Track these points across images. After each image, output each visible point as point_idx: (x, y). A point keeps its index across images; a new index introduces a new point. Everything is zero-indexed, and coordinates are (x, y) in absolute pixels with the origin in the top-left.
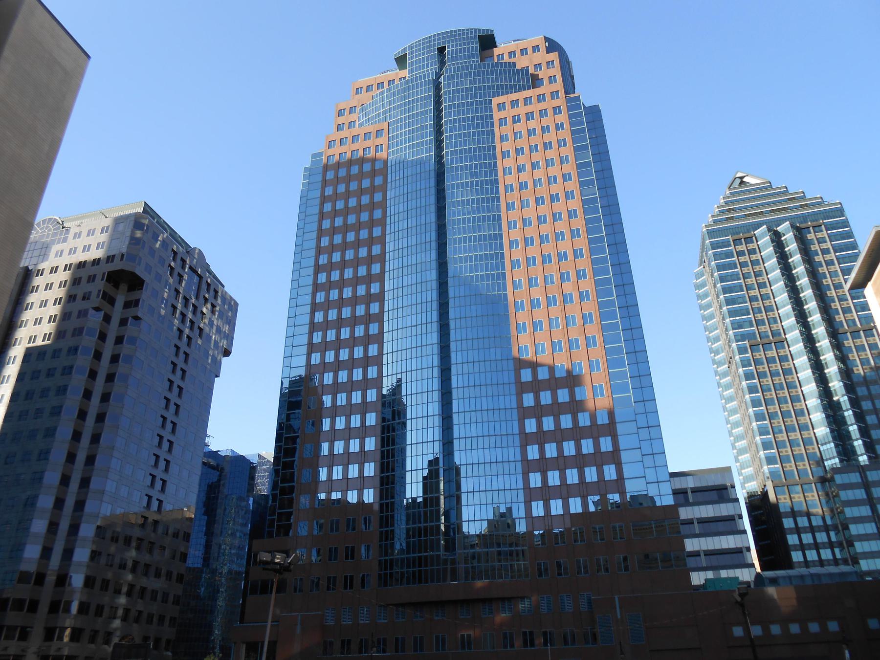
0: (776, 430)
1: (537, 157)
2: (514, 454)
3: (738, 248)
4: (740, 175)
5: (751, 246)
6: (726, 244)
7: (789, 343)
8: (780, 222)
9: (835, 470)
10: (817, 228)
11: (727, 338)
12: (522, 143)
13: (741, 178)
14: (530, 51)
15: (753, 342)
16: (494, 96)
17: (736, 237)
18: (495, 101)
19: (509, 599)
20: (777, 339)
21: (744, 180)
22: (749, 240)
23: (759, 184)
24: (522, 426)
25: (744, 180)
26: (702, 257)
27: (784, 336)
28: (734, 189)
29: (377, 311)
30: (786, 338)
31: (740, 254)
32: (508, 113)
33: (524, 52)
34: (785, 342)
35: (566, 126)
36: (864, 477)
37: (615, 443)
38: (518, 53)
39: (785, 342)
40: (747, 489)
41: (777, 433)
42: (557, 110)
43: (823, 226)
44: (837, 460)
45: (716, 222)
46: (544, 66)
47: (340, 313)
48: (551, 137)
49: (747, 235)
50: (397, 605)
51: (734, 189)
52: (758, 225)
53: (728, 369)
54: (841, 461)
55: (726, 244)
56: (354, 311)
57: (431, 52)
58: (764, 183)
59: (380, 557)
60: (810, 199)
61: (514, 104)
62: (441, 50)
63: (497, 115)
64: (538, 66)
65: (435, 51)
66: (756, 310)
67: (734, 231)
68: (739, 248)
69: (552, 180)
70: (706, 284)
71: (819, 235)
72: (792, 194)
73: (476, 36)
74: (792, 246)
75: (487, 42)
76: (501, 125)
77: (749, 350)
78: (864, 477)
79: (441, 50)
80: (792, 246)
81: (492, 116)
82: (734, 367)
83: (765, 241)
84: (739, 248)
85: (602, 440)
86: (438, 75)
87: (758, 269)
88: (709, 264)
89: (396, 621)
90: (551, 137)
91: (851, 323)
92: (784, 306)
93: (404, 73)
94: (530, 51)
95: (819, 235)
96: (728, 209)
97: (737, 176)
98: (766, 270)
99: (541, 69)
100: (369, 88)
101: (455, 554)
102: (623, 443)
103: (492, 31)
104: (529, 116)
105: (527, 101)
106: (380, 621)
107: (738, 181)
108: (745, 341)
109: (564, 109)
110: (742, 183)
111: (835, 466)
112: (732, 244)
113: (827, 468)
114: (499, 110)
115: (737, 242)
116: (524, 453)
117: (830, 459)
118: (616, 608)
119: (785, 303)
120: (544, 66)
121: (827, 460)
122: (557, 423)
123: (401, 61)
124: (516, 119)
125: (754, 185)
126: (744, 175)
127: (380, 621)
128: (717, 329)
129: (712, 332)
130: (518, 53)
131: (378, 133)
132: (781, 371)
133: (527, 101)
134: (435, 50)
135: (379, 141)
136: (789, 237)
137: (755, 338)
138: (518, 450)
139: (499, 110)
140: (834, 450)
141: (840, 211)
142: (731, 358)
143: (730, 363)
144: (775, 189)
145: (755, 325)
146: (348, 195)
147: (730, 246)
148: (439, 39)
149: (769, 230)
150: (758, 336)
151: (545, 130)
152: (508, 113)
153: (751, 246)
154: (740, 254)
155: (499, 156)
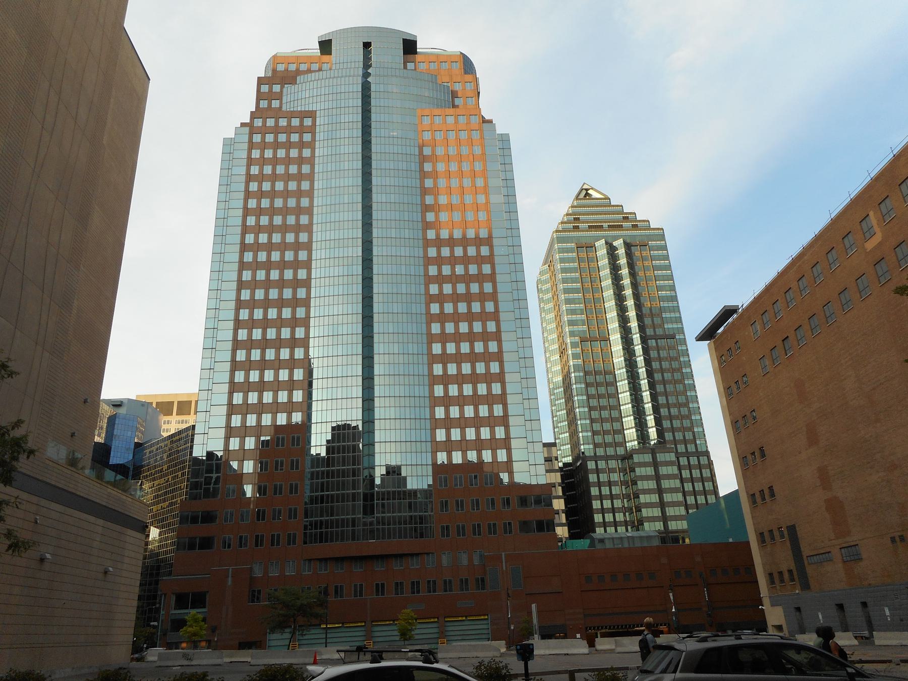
2: (425, 435)
7: (611, 342)
9: (634, 451)
13: (587, 190)
19: (417, 555)
23: (601, 199)
24: (433, 413)
25: (588, 192)
27: (608, 337)
28: (581, 199)
29: (304, 296)
30: (609, 338)
36: (654, 458)
37: (507, 432)
44: (636, 443)
47: (267, 294)
50: (320, 560)
54: (639, 443)
56: (281, 293)
62: (367, 45)
72: (626, 213)
74: (623, 261)
75: (410, 46)
78: (654, 458)
79: (367, 45)
80: (623, 261)
83: (602, 252)
85: (497, 429)
86: (366, 75)
89: (319, 572)
96: (574, 221)
97: (584, 187)
102: (513, 432)
106: (304, 573)
107: (584, 192)
111: (634, 448)
113: (628, 449)
116: (433, 435)
117: (631, 441)
118: (502, 562)
121: (628, 442)
122: (462, 412)
123: (325, 46)
126: (588, 187)
127: (304, 573)
136: (621, 252)
138: (429, 432)
140: (635, 434)
141: (662, 237)
142: (564, 349)
143: (562, 353)
144: (614, 206)
146: (274, 178)
149: (607, 243)
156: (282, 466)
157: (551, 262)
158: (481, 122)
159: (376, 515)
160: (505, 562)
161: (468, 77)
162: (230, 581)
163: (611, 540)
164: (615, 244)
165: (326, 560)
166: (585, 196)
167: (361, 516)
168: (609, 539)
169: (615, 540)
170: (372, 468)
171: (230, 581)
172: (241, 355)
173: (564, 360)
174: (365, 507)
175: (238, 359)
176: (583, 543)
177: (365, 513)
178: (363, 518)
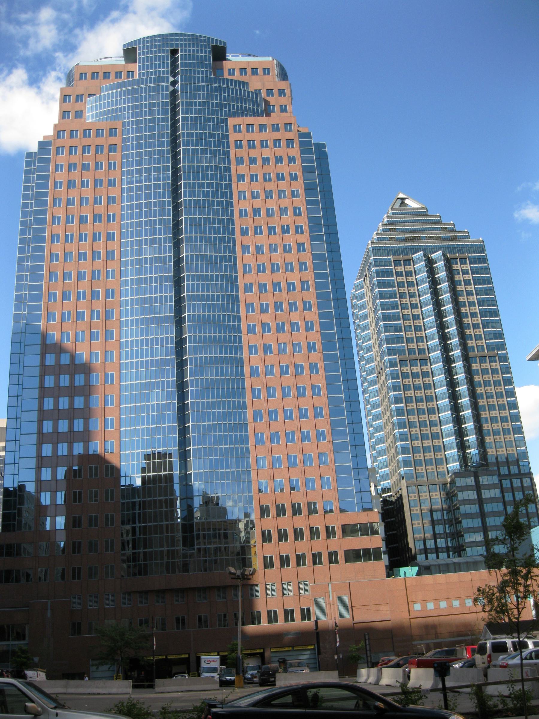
0: (413, 438)
1: (271, 186)
3: (397, 269)
4: (401, 196)
5: (408, 268)
6: (387, 263)
7: (432, 361)
8: (435, 249)
10: (463, 260)
11: (380, 351)
12: (257, 169)
13: (403, 199)
14: (260, 72)
15: (402, 357)
16: (230, 116)
17: (397, 258)
18: (232, 121)
20: (422, 356)
21: (407, 201)
22: (407, 262)
26: (363, 270)
28: (396, 209)
30: (429, 357)
31: (399, 274)
32: (244, 136)
33: (254, 71)
34: (428, 360)
35: (298, 160)
38: (249, 72)
39: (428, 360)
40: (382, 486)
41: (414, 440)
42: (290, 143)
43: (467, 260)
45: (380, 240)
46: (275, 92)
48: (284, 168)
49: (406, 257)
50: (140, 593)
51: (396, 209)
52: (415, 250)
53: (376, 378)
55: (387, 263)
57: (163, 52)
58: (422, 208)
59: (122, 550)
60: (459, 232)
61: (250, 128)
62: (174, 52)
63: (233, 137)
64: (270, 92)
65: (167, 52)
66: (407, 329)
67: (396, 252)
68: (399, 269)
69: (283, 212)
70: (364, 296)
71: (464, 267)
72: (445, 224)
73: (209, 46)
74: (442, 274)
76: (236, 147)
77: (399, 365)
79: (174, 52)
80: (442, 274)
81: (227, 136)
82: (383, 377)
84: (399, 269)
87: (412, 291)
88: (370, 279)
90: (284, 168)
91: (480, 349)
92: (431, 328)
93: (134, 67)
94: (260, 72)
95: (464, 267)
98: (418, 293)
99: (272, 95)
100: (94, 75)
101: (194, 549)
103: (224, 43)
104: (264, 144)
105: (262, 128)
107: (399, 202)
108: (395, 355)
109: (296, 143)
110: (403, 203)
112: (393, 263)
114: (235, 131)
115: (397, 262)
119: (432, 325)
120: (275, 92)
124: (251, 144)
125: (414, 209)
128: (370, 340)
129: (366, 342)
130: (249, 72)
131: (112, 132)
132: (422, 386)
133: (262, 128)
134: (167, 50)
135: (113, 140)
136: (440, 264)
137: (405, 354)
139: (235, 131)
141: (481, 249)
142: (382, 369)
143: (380, 373)
144: (431, 216)
145: (405, 342)
147: (391, 265)
148: (172, 40)
149: (425, 255)
150: (407, 352)
151: (279, 160)
152: (244, 136)
153: (408, 268)
154: (399, 274)
155: (234, 179)
156: (96, 496)
157: (366, 276)
158: (297, 131)
159: (196, 547)
160: (332, 592)
161: (283, 85)
162: (49, 614)
163: (437, 567)
164: (434, 256)
165: (146, 592)
166: (400, 206)
167: (181, 547)
168: (435, 565)
169: (441, 567)
170: (190, 498)
171: (49, 614)
172: (49, 382)
173: (382, 380)
174: (184, 538)
175: (46, 385)
176: (410, 571)
177: (184, 545)
178: (183, 550)
